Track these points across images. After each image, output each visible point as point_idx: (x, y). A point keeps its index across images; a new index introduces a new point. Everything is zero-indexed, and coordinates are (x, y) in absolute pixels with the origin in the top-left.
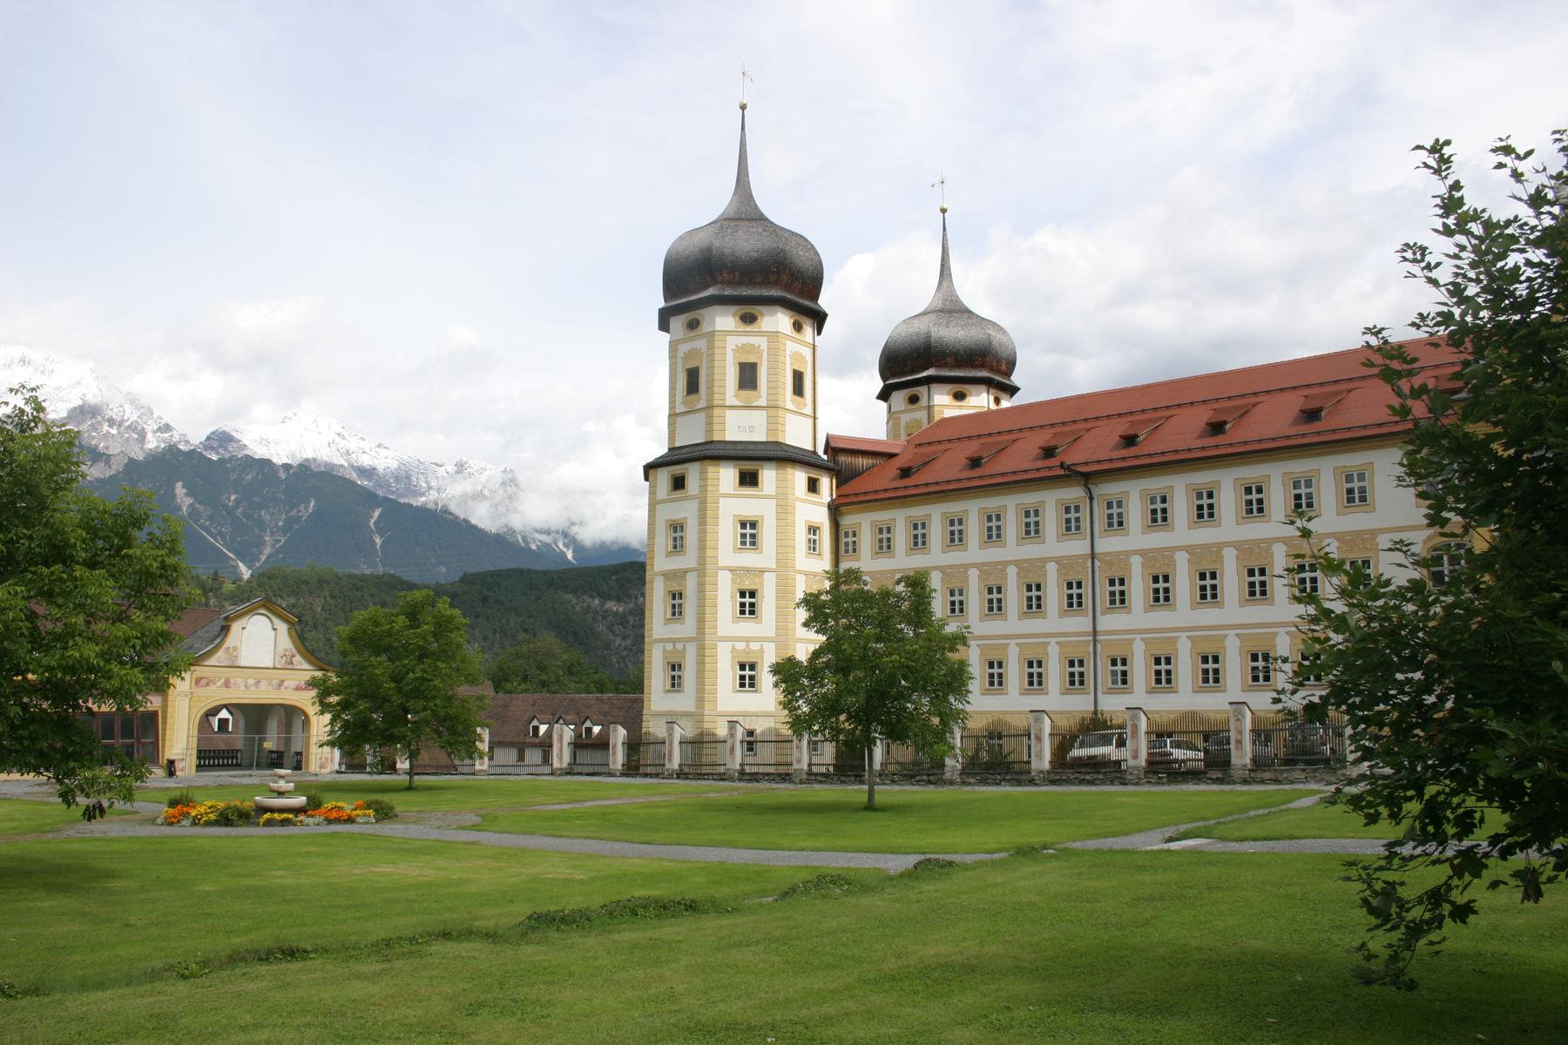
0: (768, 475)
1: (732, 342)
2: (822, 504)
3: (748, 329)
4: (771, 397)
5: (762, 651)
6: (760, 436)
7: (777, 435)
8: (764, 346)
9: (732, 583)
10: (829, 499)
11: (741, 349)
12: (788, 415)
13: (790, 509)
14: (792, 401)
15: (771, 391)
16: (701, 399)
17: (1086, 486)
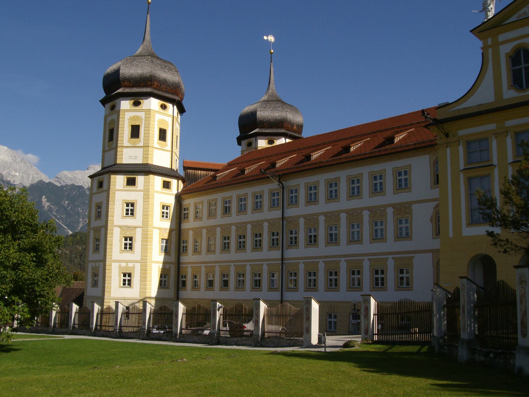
0: (140, 179)
2: (172, 194)
3: (136, 108)
4: (146, 142)
5: (134, 267)
6: (139, 161)
7: (148, 160)
8: (143, 117)
9: (121, 233)
10: (176, 192)
11: (132, 119)
12: (155, 150)
13: (151, 196)
14: (158, 143)
15: (145, 139)
16: (113, 143)
17: (280, 182)
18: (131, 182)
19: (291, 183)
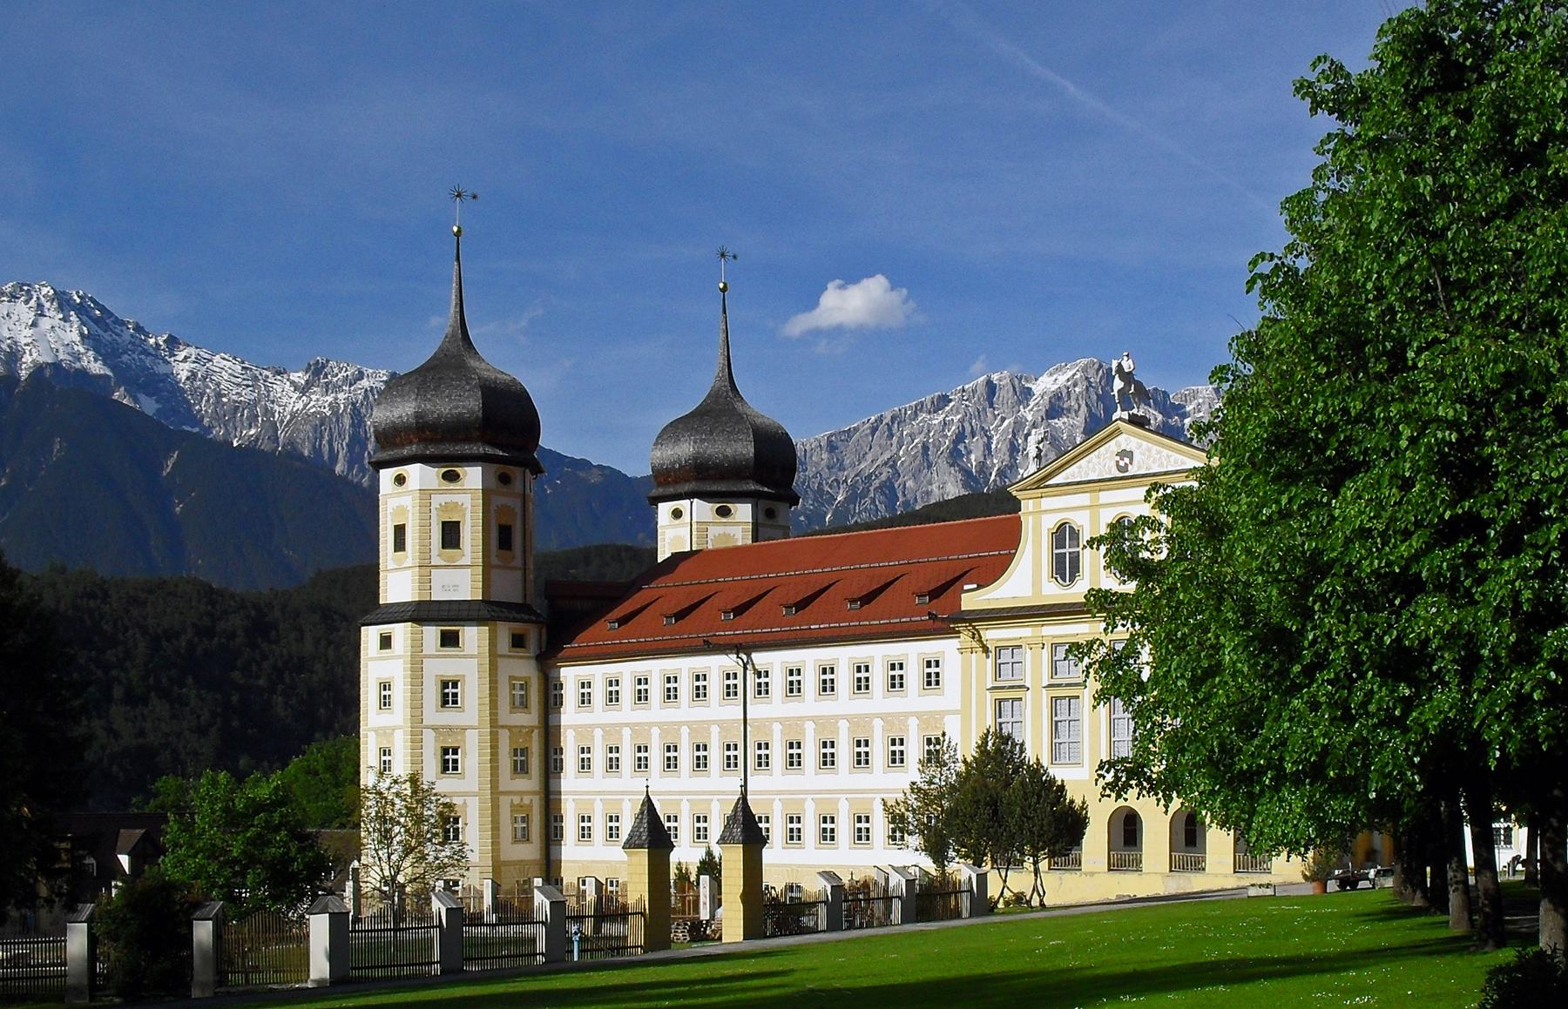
1: (437, 500)
3: (452, 486)
8: (468, 505)
11: (446, 507)
18: (449, 640)
19: (760, 659)
